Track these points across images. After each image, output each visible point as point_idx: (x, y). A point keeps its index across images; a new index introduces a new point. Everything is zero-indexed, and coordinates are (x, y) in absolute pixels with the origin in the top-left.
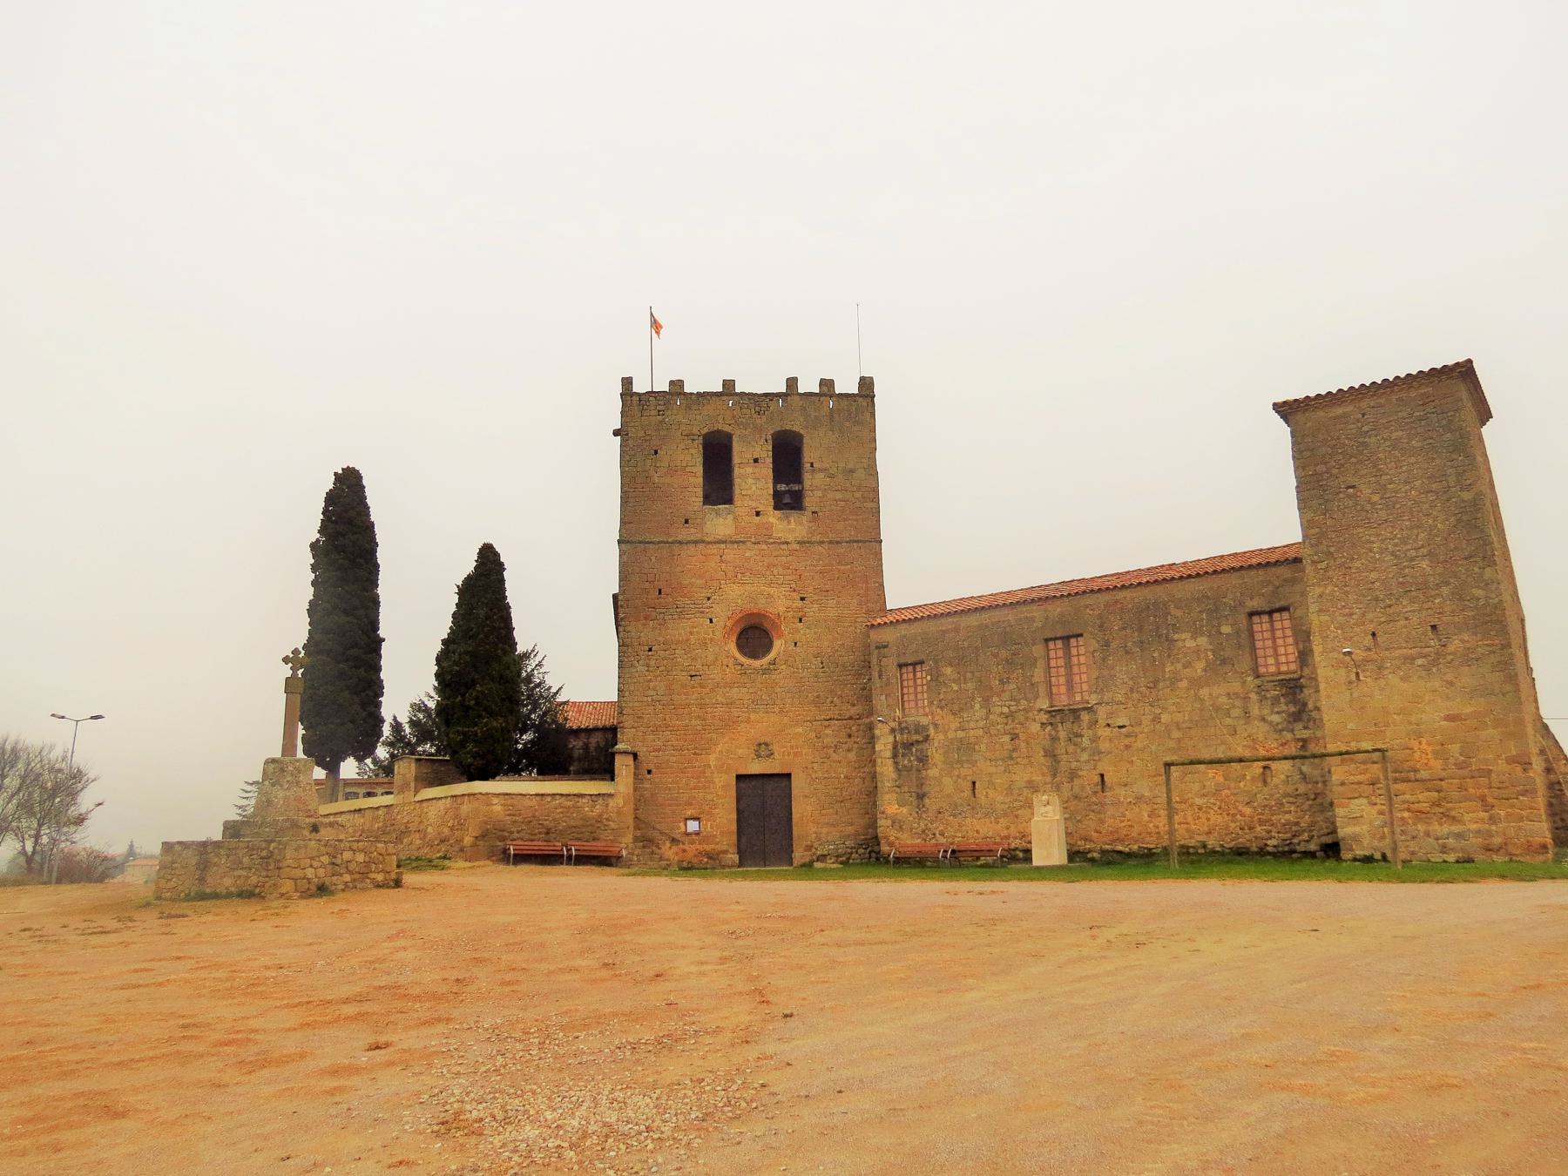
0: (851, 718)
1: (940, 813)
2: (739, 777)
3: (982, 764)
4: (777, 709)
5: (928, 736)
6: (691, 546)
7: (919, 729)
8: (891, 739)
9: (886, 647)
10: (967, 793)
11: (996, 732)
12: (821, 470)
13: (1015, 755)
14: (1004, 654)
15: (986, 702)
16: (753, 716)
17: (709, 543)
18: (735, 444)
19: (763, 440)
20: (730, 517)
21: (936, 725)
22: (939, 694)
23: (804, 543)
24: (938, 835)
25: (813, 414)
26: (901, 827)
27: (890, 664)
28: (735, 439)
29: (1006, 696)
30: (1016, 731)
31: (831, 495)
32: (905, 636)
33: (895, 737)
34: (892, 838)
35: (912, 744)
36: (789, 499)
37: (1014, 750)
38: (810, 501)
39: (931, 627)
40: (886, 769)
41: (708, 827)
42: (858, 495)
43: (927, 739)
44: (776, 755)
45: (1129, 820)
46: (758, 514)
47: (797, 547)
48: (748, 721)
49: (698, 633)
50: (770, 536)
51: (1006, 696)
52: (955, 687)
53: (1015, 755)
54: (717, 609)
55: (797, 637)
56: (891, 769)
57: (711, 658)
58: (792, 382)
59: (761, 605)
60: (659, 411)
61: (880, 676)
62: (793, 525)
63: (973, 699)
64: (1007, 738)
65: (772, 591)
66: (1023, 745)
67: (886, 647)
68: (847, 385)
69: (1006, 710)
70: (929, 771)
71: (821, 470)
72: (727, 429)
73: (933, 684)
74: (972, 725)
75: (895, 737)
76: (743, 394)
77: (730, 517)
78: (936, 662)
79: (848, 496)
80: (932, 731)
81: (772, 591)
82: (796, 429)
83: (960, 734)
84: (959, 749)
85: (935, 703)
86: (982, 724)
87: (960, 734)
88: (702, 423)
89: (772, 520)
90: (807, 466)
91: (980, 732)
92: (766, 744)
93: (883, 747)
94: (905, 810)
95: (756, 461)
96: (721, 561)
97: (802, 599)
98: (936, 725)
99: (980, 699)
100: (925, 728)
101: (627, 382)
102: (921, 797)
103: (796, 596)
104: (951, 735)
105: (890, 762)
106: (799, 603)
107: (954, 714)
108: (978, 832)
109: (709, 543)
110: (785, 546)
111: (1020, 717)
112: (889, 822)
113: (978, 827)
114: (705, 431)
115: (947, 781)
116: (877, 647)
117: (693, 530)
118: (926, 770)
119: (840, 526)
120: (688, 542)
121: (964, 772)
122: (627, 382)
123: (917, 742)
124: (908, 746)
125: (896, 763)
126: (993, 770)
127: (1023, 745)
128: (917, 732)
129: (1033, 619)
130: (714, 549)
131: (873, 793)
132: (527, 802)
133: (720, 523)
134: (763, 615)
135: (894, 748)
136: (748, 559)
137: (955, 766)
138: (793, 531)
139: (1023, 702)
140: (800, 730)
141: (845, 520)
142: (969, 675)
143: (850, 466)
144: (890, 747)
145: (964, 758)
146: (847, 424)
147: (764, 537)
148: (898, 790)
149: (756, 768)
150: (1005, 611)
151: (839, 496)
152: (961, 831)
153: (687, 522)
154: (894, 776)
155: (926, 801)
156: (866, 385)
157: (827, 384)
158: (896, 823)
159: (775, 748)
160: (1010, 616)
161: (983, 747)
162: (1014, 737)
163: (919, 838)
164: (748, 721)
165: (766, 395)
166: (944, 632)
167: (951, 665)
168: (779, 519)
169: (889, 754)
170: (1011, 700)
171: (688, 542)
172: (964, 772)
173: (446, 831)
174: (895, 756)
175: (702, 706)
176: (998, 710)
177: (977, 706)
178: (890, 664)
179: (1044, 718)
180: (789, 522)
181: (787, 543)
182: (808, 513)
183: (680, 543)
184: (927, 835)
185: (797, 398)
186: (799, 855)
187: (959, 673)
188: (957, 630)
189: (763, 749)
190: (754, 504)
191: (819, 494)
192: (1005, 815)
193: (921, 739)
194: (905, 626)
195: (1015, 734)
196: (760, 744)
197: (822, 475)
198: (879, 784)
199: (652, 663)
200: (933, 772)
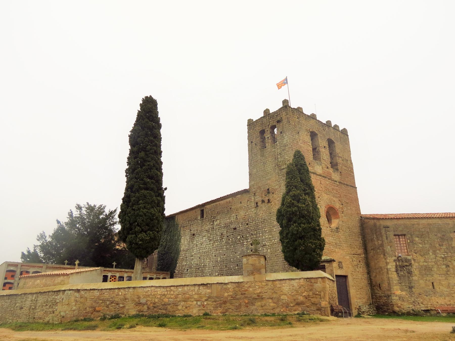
0: (359, 255)
1: (420, 294)
3: (436, 276)
5: (411, 263)
7: (407, 260)
8: (394, 264)
9: (388, 227)
10: (431, 287)
11: (440, 264)
13: (449, 273)
14: (439, 235)
15: (434, 253)
20: (321, 167)
21: (414, 260)
22: (414, 247)
24: (420, 304)
26: (403, 300)
27: (391, 234)
29: (442, 251)
30: (448, 264)
32: (396, 224)
33: (396, 263)
34: (399, 305)
35: (404, 266)
36: (334, 165)
37: (448, 271)
43: (410, 264)
44: (344, 268)
47: (338, 183)
48: (335, 252)
51: (442, 251)
52: (421, 246)
53: (449, 273)
56: (396, 276)
60: (298, 117)
61: (387, 238)
62: (336, 175)
63: (429, 251)
64: (444, 267)
66: (451, 269)
67: (388, 227)
69: (443, 256)
70: (413, 278)
72: (317, 132)
73: (411, 243)
74: (430, 261)
75: (396, 263)
76: (319, 121)
78: (411, 235)
80: (413, 262)
83: (425, 264)
84: (425, 269)
85: (413, 251)
86: (434, 260)
87: (425, 264)
91: (433, 263)
92: (341, 262)
93: (391, 267)
94: (404, 293)
95: (325, 147)
97: (342, 204)
98: (414, 260)
99: (432, 251)
100: (409, 260)
102: (411, 288)
104: (421, 264)
105: (395, 273)
106: (341, 206)
107: (422, 256)
108: (437, 302)
111: (449, 259)
112: (397, 298)
113: (438, 301)
115: (421, 282)
116: (384, 227)
118: (412, 277)
121: (428, 278)
123: (406, 266)
124: (402, 267)
125: (398, 274)
126: (440, 278)
127: (451, 269)
128: (406, 262)
129: (449, 224)
134: (332, 207)
137: (424, 276)
139: (449, 253)
140: (348, 257)
141: (348, 178)
142: (426, 242)
144: (394, 267)
145: (428, 273)
148: (400, 285)
150: (438, 220)
151: (345, 168)
152: (430, 302)
154: (397, 279)
155: (413, 289)
158: (401, 298)
160: (440, 222)
161: (435, 269)
162: (448, 266)
163: (411, 304)
166: (413, 224)
167: (418, 237)
169: (394, 270)
170: (445, 252)
172: (428, 278)
173: (301, 299)
174: (397, 271)
176: (440, 255)
177: (431, 254)
178: (391, 234)
184: (415, 303)
185: (332, 128)
186: (355, 312)
187: (421, 240)
192: (448, 296)
193: (408, 265)
195: (447, 265)
196: (339, 262)
198: (391, 282)
200: (415, 278)
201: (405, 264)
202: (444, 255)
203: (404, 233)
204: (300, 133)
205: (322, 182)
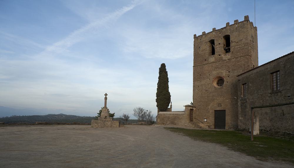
2: (215, 111)
4: (223, 96)
6: (206, 65)
12: (234, 42)
16: (218, 98)
17: (209, 64)
18: (215, 41)
19: (221, 39)
23: (229, 59)
25: (232, 30)
28: (215, 40)
31: (237, 47)
36: (227, 50)
38: (232, 50)
39: (247, 74)
40: (240, 109)
41: (208, 120)
42: (243, 45)
43: (246, 101)
44: (222, 106)
45: (290, 124)
46: (220, 55)
47: (228, 61)
48: (217, 99)
49: (207, 82)
50: (222, 60)
54: (211, 77)
55: (228, 81)
56: (240, 109)
57: (210, 87)
58: (228, 24)
59: (220, 75)
61: (239, 87)
65: (222, 71)
68: (241, 19)
69: (261, 94)
71: (234, 42)
74: (255, 98)
77: (214, 57)
79: (241, 46)
81: (222, 71)
82: (228, 34)
88: (208, 39)
89: (222, 56)
90: (231, 42)
92: (220, 104)
95: (219, 44)
96: (212, 67)
97: (229, 72)
98: (248, 98)
101: (195, 35)
103: (227, 71)
104: (251, 100)
106: (228, 73)
109: (209, 64)
110: (225, 61)
114: (209, 41)
117: (207, 62)
119: (238, 54)
120: (205, 64)
122: (195, 35)
124: (243, 103)
130: (210, 65)
131: (237, 116)
132: (168, 115)
133: (212, 59)
135: (241, 104)
136: (217, 65)
138: (227, 57)
140: (227, 101)
143: (241, 39)
146: (241, 29)
147: (221, 59)
149: (218, 109)
151: (238, 47)
153: (205, 60)
156: (247, 18)
157: (236, 21)
159: (222, 105)
164: (217, 99)
165: (221, 29)
166: (250, 75)
167: (251, 83)
168: (224, 55)
171: (205, 64)
175: (208, 97)
179: (269, 95)
180: (226, 56)
181: (226, 60)
182: (231, 53)
183: (204, 65)
188: (252, 74)
189: (219, 105)
190: (219, 53)
191: (233, 47)
194: (243, 75)
196: (219, 104)
197: (234, 43)
199: (199, 89)
200: (247, 110)
201: (245, 101)
202: (262, 93)
203: (245, 82)
204: (200, 47)
205: (213, 66)
